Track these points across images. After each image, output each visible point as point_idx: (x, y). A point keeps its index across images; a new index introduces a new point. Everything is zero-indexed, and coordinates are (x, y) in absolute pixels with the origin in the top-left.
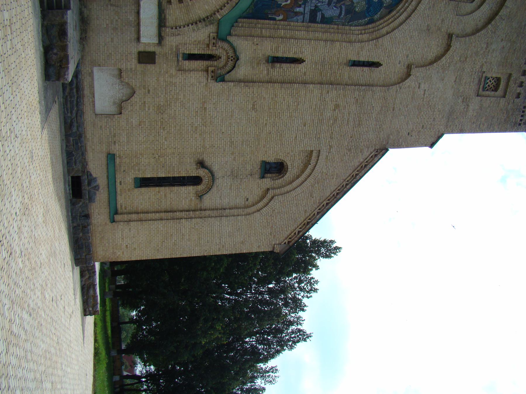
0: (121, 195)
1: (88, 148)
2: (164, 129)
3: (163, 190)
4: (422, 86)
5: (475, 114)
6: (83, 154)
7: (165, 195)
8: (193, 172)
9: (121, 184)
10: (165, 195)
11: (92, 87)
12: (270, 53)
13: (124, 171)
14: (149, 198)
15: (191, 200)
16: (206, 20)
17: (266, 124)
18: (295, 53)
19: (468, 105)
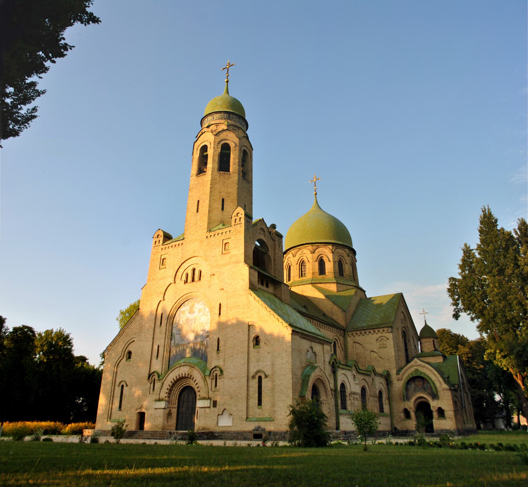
0: (264, 415)
1: (243, 430)
2: (238, 395)
3: (257, 395)
4: (226, 281)
5: (237, 250)
6: (245, 432)
7: (265, 393)
8: (257, 380)
9: (259, 415)
10: (265, 393)
11: (222, 427)
12: (216, 353)
13: (255, 413)
14: (266, 401)
15: (268, 380)
16: (205, 380)
17: (238, 350)
18: (216, 342)
19: (233, 255)
